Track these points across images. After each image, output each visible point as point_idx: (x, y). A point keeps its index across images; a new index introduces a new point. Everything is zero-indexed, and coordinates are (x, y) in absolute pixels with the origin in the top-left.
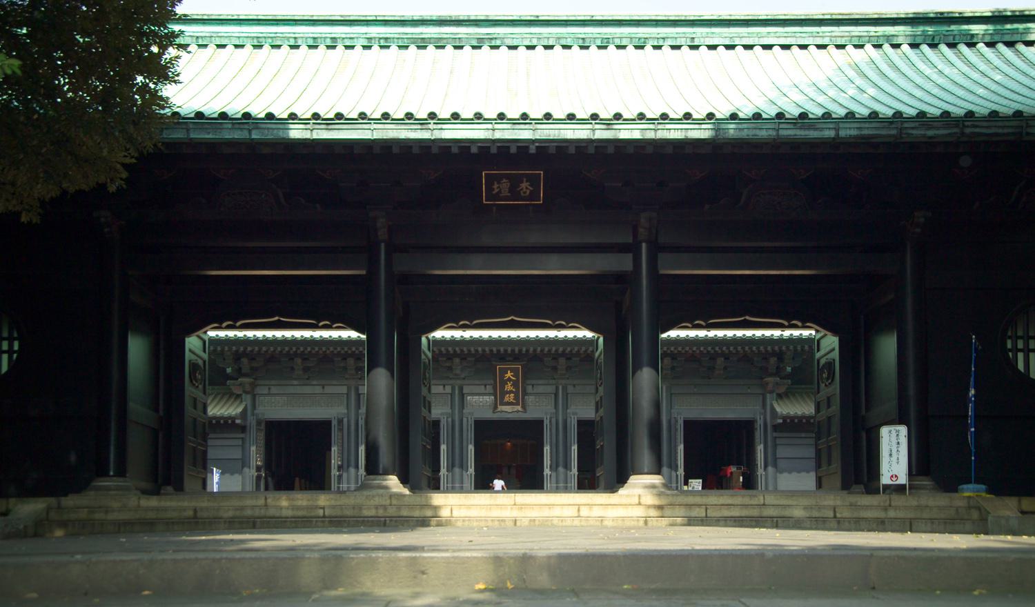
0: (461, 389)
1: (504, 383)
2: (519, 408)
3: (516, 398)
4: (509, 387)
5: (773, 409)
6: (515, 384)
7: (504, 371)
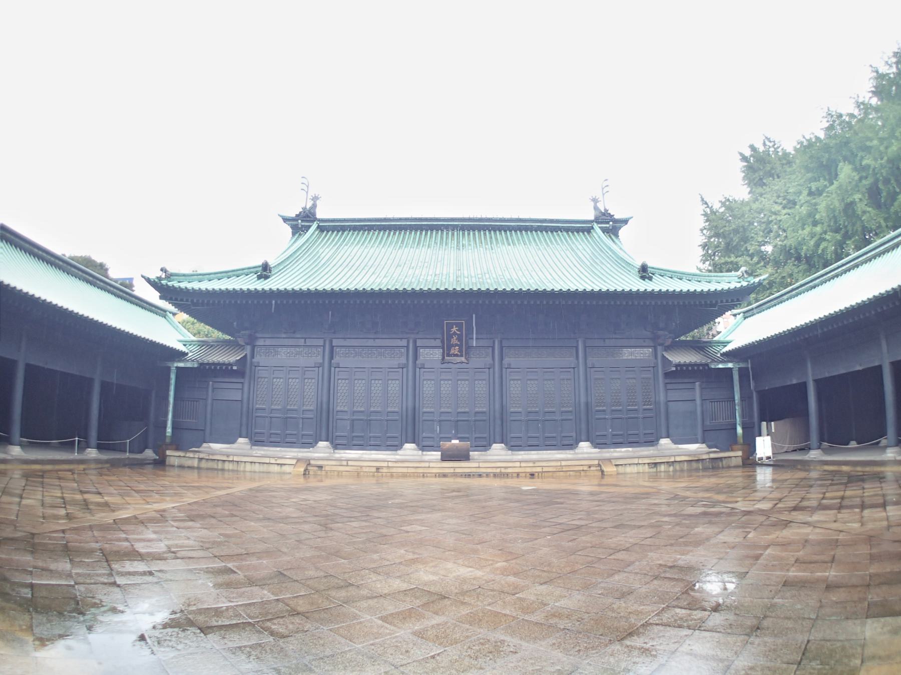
0: (415, 342)
1: (450, 337)
2: (463, 359)
3: (460, 351)
4: (454, 340)
5: (663, 357)
6: (460, 338)
7: (450, 326)
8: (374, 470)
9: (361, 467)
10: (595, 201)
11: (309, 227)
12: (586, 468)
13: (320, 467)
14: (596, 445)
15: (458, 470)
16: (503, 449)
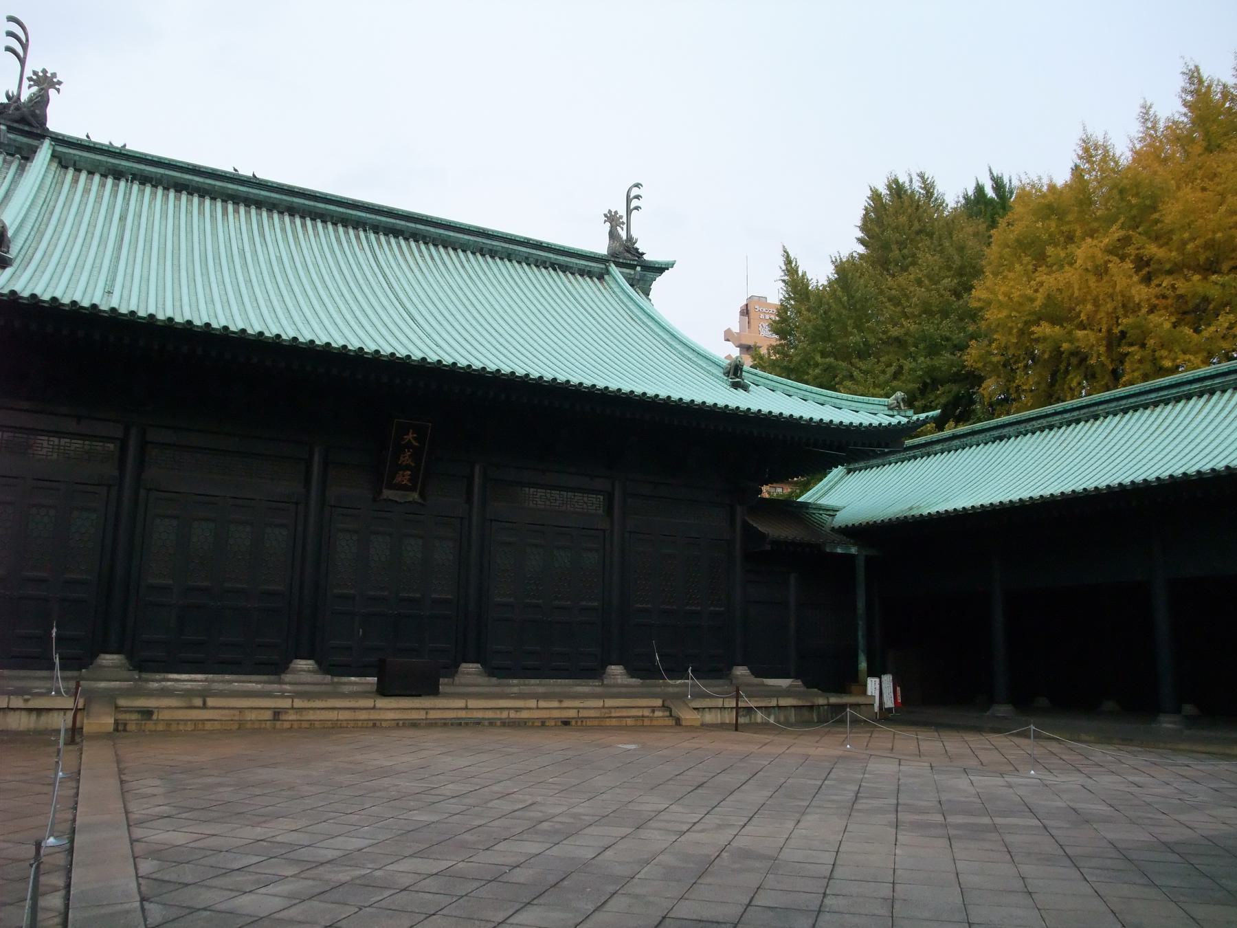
2: (415, 496)
4: (406, 458)
5: (746, 525)
8: (268, 715)
9: (241, 710)
10: (612, 219)
11: (34, 151)
12: (647, 713)
13: (147, 713)
14: (632, 672)
15: (433, 715)
16: (479, 674)
